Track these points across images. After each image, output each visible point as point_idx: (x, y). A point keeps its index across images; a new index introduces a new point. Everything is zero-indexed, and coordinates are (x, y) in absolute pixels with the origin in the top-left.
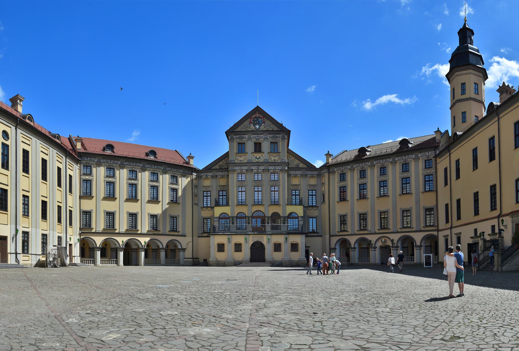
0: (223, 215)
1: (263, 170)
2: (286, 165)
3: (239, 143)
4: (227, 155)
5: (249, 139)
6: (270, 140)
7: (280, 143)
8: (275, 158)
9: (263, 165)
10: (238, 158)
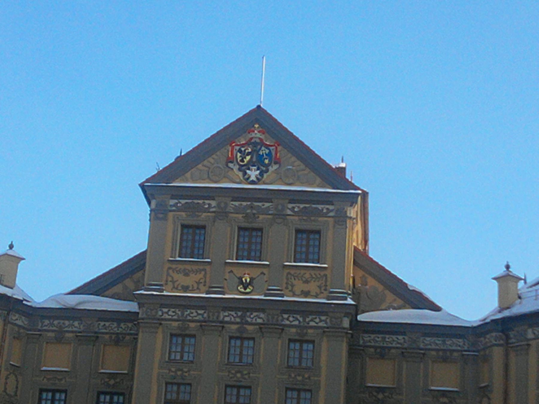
1: (261, 327)
2: (347, 315)
3: (184, 226)
4: (136, 266)
5: (222, 214)
6: (295, 221)
7: (330, 234)
8: (306, 287)
9: (263, 310)
10: (176, 276)
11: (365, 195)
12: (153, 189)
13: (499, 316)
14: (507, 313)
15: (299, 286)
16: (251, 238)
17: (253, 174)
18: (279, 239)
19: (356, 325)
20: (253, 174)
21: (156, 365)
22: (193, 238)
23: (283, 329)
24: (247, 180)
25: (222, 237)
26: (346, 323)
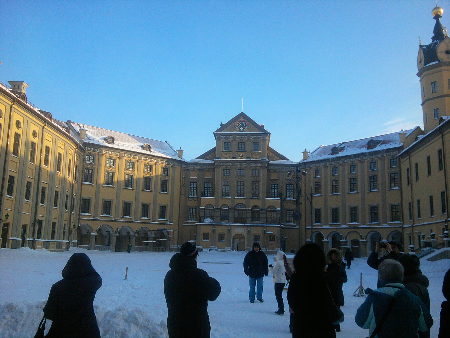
0: (209, 206)
1: (246, 167)
5: (234, 139)
8: (256, 157)
10: (224, 155)
11: (270, 133)
12: (216, 134)
13: (304, 162)
14: (305, 161)
15: (255, 157)
16: (242, 145)
17: (242, 129)
18: (249, 145)
19: (268, 164)
20: (242, 129)
21: (220, 176)
22: (227, 145)
23: (251, 167)
24: (240, 131)
25: (235, 144)
26: (266, 165)
